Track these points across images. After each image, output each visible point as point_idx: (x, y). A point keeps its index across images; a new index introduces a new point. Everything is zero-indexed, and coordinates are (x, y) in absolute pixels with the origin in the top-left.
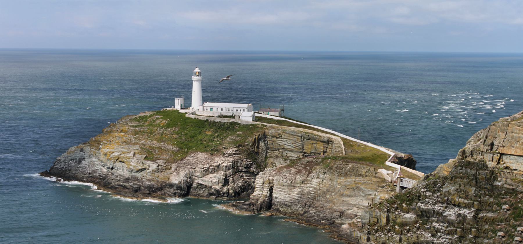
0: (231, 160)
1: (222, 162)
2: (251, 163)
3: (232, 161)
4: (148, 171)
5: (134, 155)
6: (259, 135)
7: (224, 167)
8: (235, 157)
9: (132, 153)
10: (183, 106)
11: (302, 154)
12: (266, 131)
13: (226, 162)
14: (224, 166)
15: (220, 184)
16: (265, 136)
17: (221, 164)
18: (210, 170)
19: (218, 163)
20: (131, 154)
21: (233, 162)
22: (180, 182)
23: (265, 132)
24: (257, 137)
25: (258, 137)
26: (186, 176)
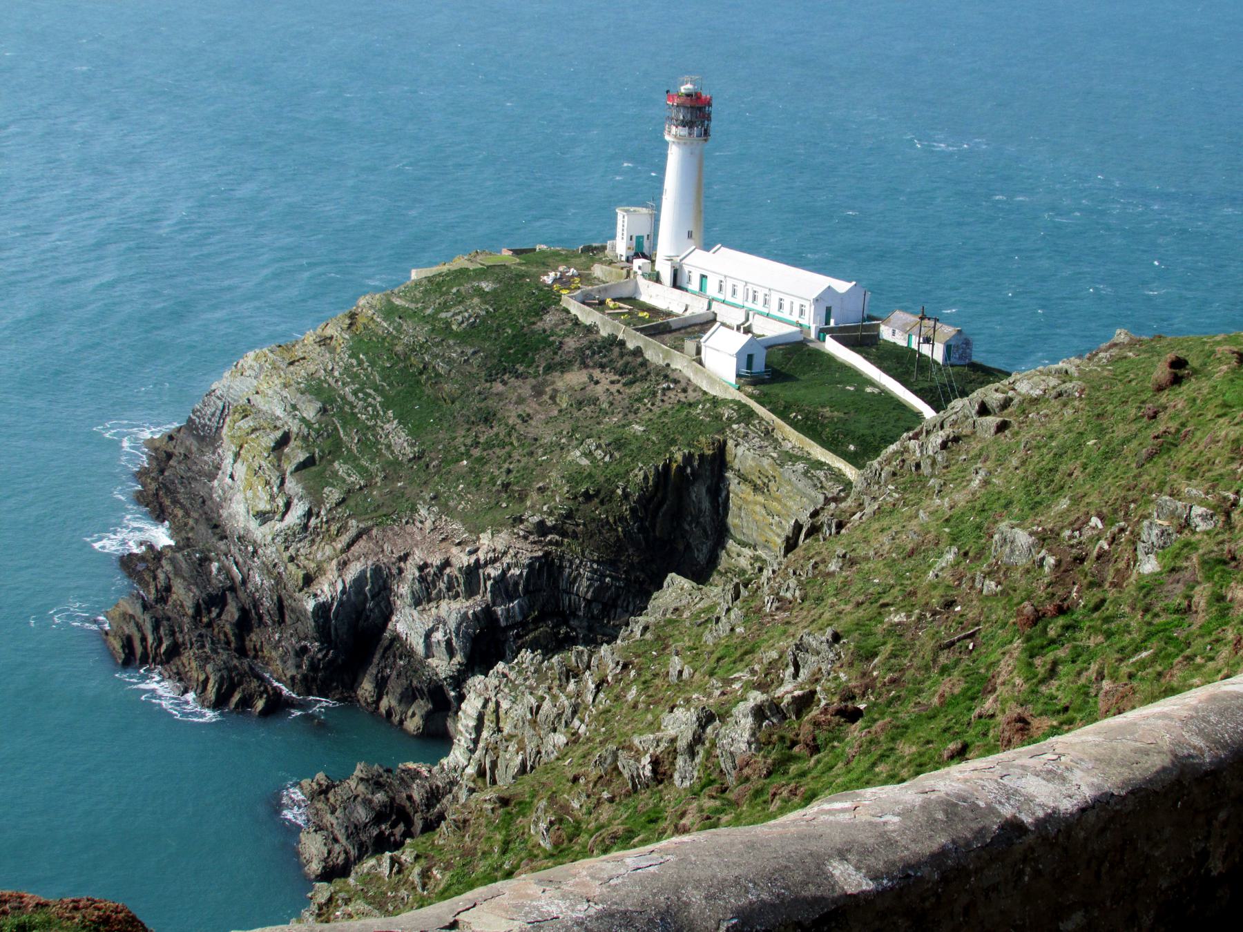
0: (528, 552)
1: (491, 555)
2: (622, 584)
3: (527, 562)
4: (279, 526)
6: (688, 459)
7: (489, 583)
8: (550, 543)
9: (279, 434)
10: (646, 244)
12: (730, 443)
13: (507, 560)
15: (459, 658)
16: (718, 461)
17: (486, 564)
18: (442, 586)
19: (472, 560)
20: (270, 439)
21: (530, 566)
22: (322, 609)
23: (722, 448)
24: (674, 466)
25: (681, 469)
26: (360, 581)
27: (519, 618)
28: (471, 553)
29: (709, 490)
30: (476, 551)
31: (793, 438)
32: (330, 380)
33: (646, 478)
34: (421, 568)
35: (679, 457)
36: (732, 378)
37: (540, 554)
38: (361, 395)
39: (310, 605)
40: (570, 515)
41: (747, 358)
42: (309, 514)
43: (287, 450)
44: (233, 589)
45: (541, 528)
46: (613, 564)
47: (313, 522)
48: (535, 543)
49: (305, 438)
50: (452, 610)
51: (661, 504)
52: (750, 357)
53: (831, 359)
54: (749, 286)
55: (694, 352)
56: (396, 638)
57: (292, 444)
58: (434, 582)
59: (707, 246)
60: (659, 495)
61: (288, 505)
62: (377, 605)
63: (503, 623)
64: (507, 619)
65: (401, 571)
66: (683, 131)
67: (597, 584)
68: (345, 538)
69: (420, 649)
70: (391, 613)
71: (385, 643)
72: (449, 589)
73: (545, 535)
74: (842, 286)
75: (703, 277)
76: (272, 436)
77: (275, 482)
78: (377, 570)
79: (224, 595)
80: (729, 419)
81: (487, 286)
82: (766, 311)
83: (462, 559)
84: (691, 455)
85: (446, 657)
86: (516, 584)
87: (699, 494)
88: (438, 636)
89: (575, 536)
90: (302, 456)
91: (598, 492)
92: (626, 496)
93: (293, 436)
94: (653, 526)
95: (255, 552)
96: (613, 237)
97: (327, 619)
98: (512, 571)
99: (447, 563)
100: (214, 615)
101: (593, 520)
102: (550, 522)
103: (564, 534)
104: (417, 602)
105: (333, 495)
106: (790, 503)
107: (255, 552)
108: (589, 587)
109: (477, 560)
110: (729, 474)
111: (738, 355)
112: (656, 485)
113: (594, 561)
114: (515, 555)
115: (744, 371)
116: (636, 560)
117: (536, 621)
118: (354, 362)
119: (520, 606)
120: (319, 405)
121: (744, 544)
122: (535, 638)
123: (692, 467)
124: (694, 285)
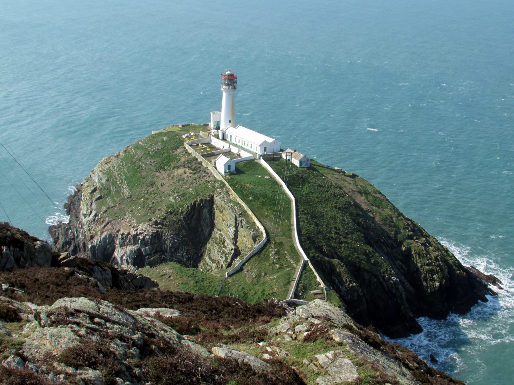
0: (152, 230)
1: (141, 231)
3: (151, 234)
5: (94, 190)
6: (202, 200)
7: (140, 241)
8: (159, 228)
9: (93, 188)
11: (233, 247)
12: (215, 196)
13: (145, 233)
14: (139, 239)
16: (211, 201)
18: (128, 241)
21: (152, 235)
22: (93, 247)
23: (212, 198)
25: (199, 204)
26: (105, 238)
27: (149, 252)
28: (135, 231)
29: (208, 211)
30: (137, 230)
31: (234, 195)
32: (113, 170)
33: (188, 207)
34: (122, 235)
35: (199, 200)
36: (223, 173)
37: (155, 231)
38: (119, 175)
39: (90, 246)
40: (165, 219)
41: (228, 166)
42: (96, 215)
43: (95, 193)
44: (74, 239)
45: (156, 223)
46: (178, 235)
47: (97, 218)
48: (154, 228)
49: (101, 190)
50: (130, 248)
51: (193, 216)
52: (229, 166)
53: (260, 165)
54: (243, 140)
55: (214, 164)
56: (115, 258)
57: (97, 191)
58: (125, 239)
59: (235, 126)
60: (192, 213)
61: (91, 212)
62: (111, 246)
63: (144, 254)
64: (145, 253)
65: (117, 235)
66: (226, 87)
67: (172, 242)
68: (104, 224)
69: (120, 261)
70: (115, 249)
71: (112, 259)
72: (129, 242)
73: (157, 225)
74: (270, 140)
75: (231, 136)
76: (91, 189)
77: (89, 204)
78: (110, 235)
79: (71, 241)
80: (217, 187)
81: (165, 139)
82: (247, 148)
83: (133, 233)
84: (202, 200)
85: (127, 265)
86: (148, 241)
87: (205, 212)
88: (124, 258)
89: (166, 226)
90: (98, 196)
91: (174, 211)
92: (182, 213)
93: (97, 189)
94: (191, 223)
95: (82, 227)
96: (210, 121)
97: (95, 251)
98: (147, 237)
99: (129, 234)
100: (67, 248)
101: (172, 220)
102: (159, 221)
103: (163, 225)
104: (121, 246)
105: (104, 209)
106: (228, 217)
107: (82, 227)
108: (170, 242)
109: (137, 233)
110: (214, 206)
111: (225, 165)
112: (191, 209)
113: (172, 234)
114: (148, 232)
115: (227, 170)
116: (185, 234)
117: (155, 253)
118: (121, 164)
119: (149, 249)
120: (107, 178)
121: (218, 230)
122: (154, 259)
123: (203, 204)
124: (229, 139)
